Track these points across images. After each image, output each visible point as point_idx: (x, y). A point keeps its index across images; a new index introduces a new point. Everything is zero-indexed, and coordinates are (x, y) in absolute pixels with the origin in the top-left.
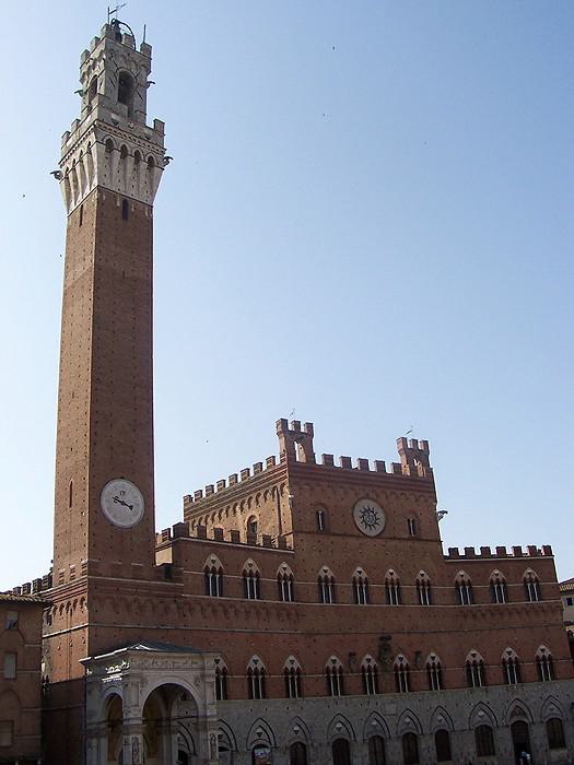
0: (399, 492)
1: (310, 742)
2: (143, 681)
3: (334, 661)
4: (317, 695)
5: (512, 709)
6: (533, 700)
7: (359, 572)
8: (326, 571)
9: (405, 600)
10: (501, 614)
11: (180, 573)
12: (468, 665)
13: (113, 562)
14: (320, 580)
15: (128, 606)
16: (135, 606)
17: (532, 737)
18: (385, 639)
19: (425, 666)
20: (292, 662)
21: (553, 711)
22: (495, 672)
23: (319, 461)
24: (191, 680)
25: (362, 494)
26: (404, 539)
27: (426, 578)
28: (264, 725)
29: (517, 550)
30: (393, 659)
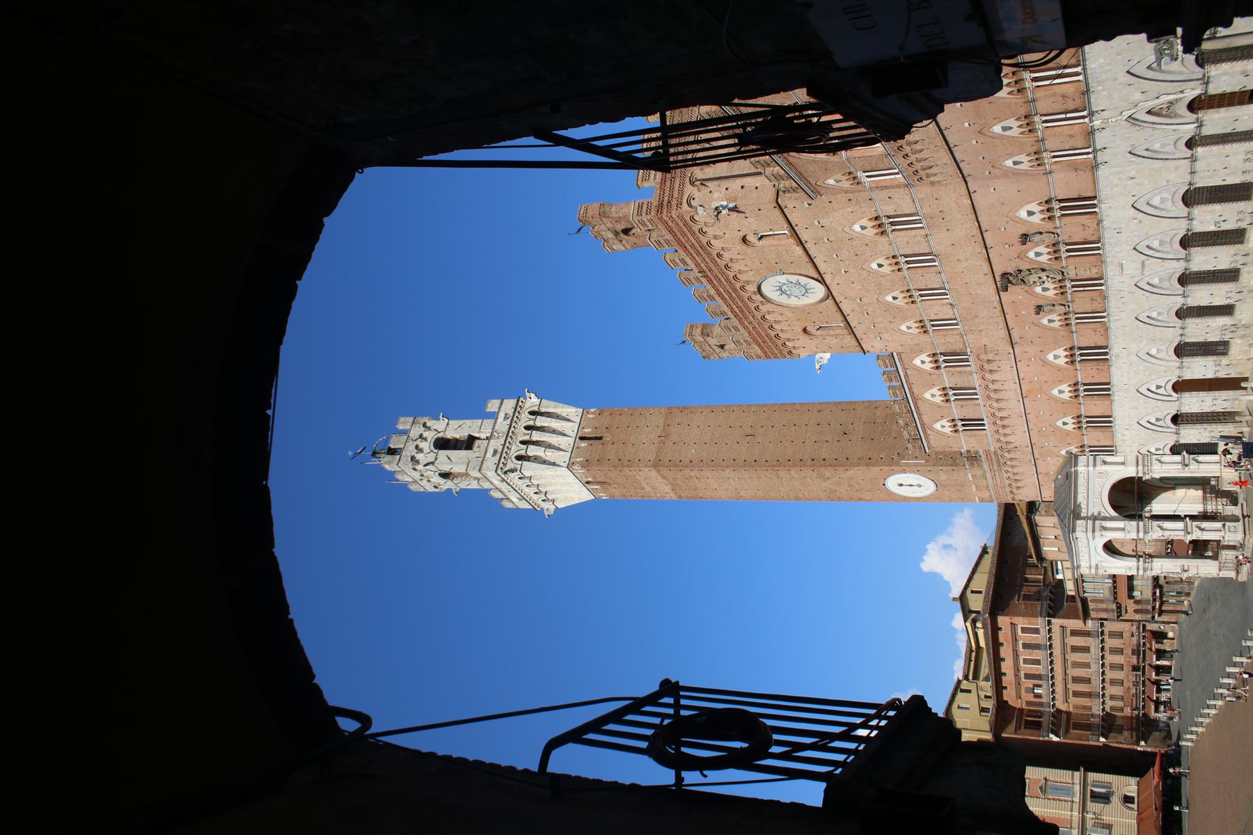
18: (1006, 281)
19: (1049, 226)
20: (1058, 356)
25: (758, 297)
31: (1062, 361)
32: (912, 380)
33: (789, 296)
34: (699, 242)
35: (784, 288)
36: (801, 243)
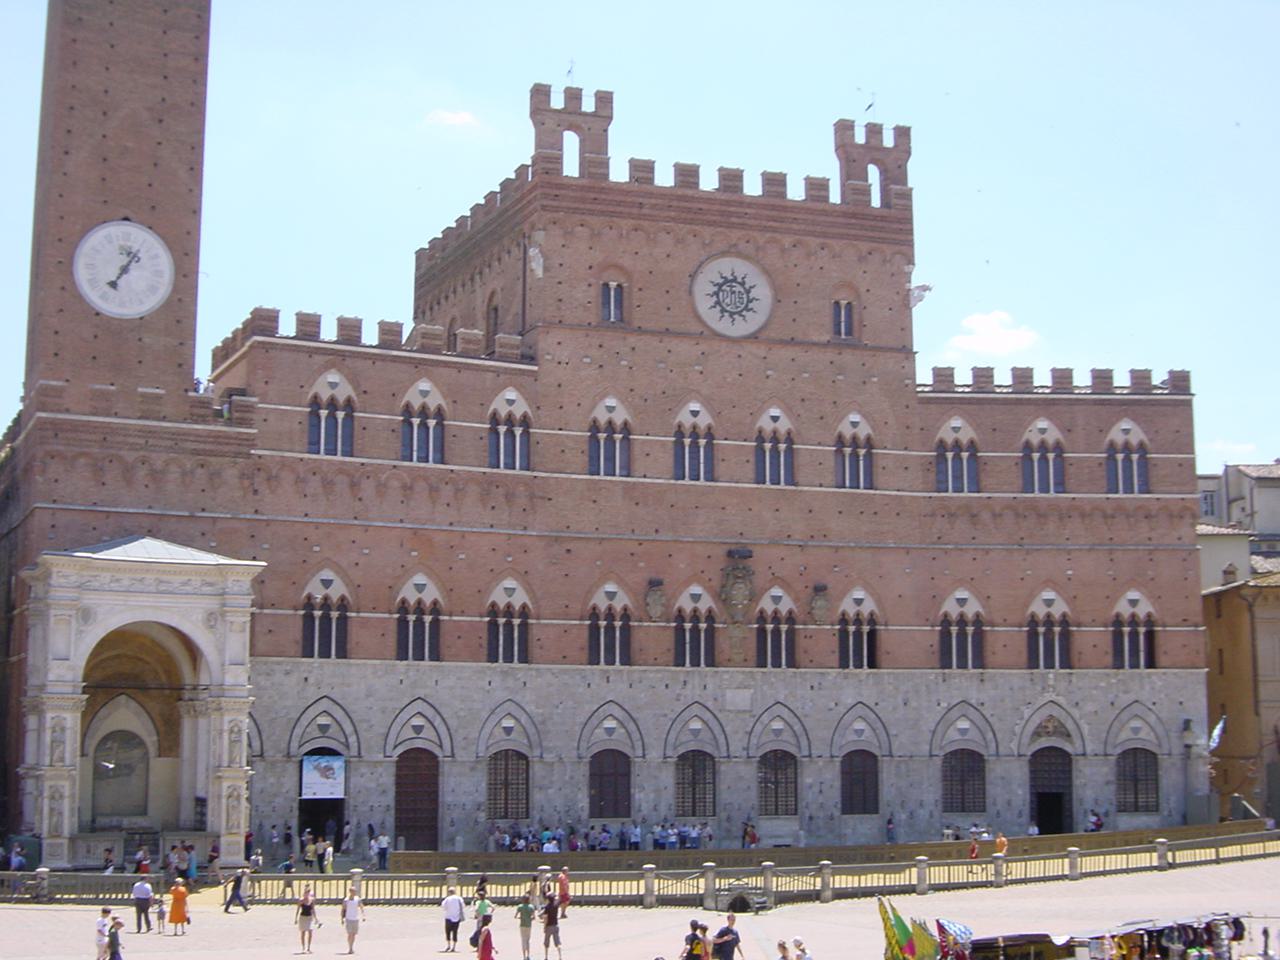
0: (813, 242)
1: (537, 752)
2: (86, 615)
3: (611, 595)
4: (565, 659)
5: (1036, 720)
6: (1090, 707)
7: (693, 413)
8: (612, 409)
9: (800, 477)
10: (1042, 516)
11: (250, 408)
12: (946, 622)
13: (98, 387)
14: (595, 428)
15: (128, 472)
16: (142, 472)
17: (1077, 782)
19: (838, 615)
20: (510, 592)
21: (1141, 733)
22: (1006, 638)
23: (619, 173)
24: (199, 616)
26: (815, 344)
27: (864, 431)
28: (430, 712)
29: (1102, 378)
30: (754, 597)
31: (500, 598)
32: (465, 374)
33: (720, 286)
34: (856, 238)
35: (738, 288)
36: (840, 346)
